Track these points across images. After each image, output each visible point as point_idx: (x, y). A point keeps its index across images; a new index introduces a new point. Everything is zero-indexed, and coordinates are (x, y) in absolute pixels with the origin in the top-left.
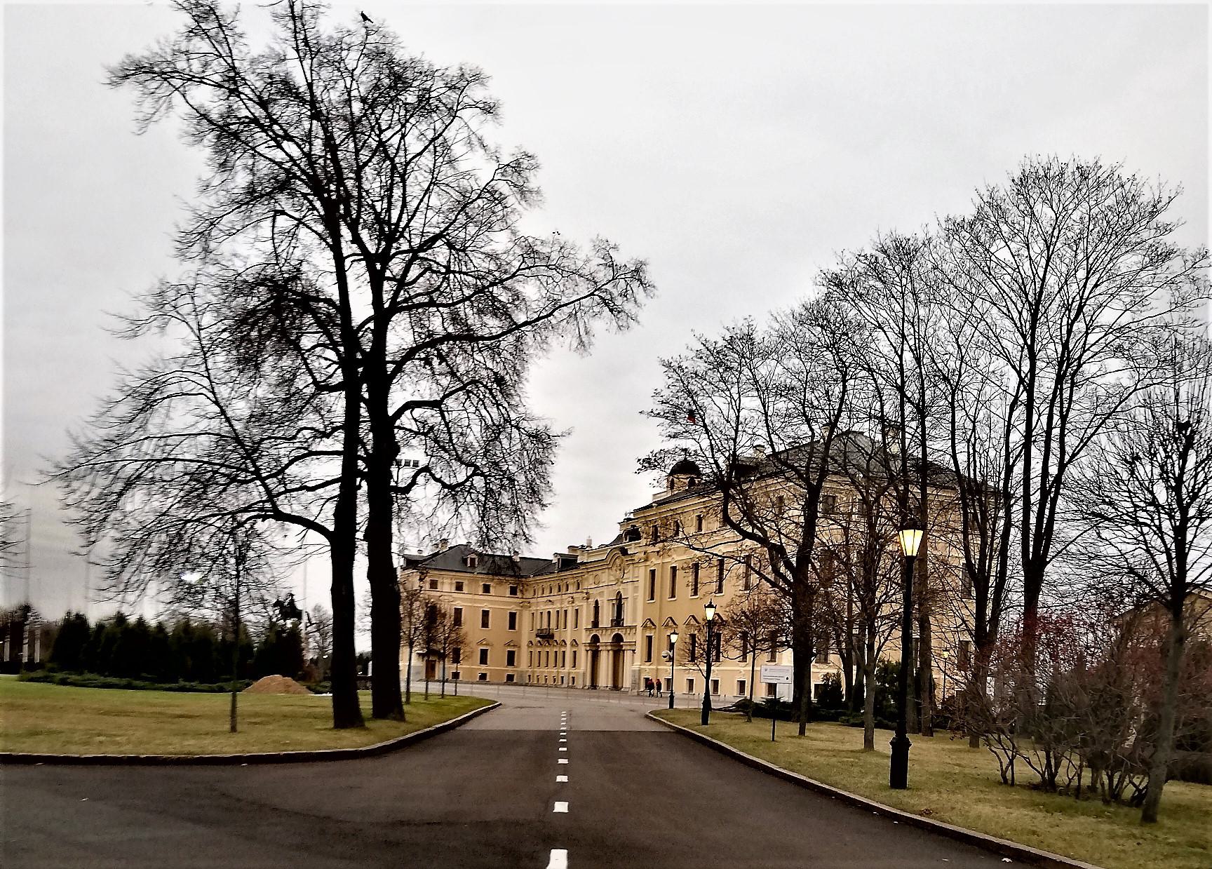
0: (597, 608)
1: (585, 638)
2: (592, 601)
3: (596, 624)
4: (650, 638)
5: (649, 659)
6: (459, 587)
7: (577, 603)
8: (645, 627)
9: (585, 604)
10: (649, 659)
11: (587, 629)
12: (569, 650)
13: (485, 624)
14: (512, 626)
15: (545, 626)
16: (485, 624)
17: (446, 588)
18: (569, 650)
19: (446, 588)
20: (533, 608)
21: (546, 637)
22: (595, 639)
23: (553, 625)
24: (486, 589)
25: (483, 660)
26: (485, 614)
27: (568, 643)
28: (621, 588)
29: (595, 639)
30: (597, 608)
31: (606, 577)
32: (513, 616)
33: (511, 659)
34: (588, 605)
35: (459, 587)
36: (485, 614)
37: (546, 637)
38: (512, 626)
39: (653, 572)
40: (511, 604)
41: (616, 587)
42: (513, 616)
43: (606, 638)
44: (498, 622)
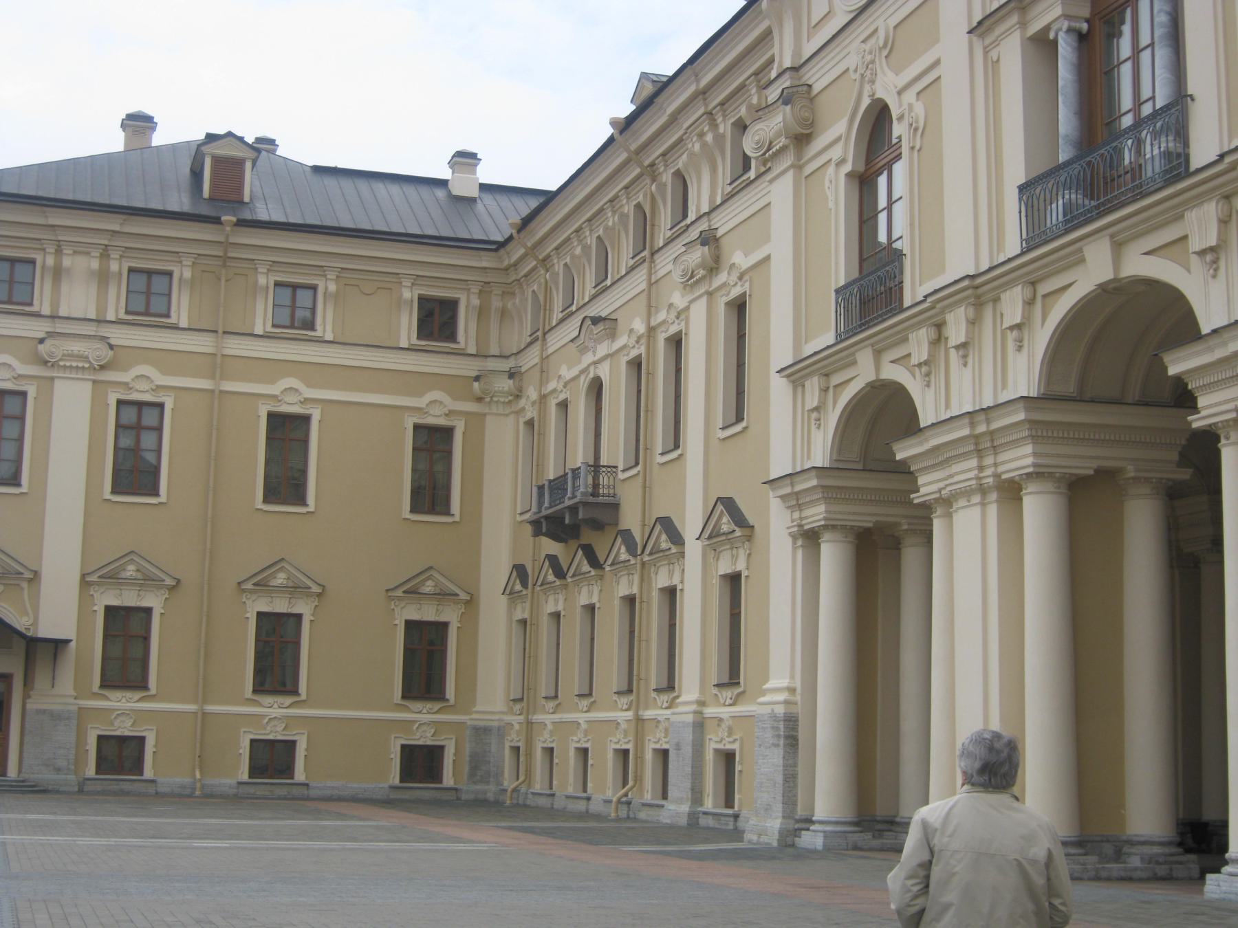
1: (794, 435)
12: (694, 576)
13: (286, 484)
14: (430, 495)
16: (286, 484)
17: (78, 298)
18: (694, 576)
19: (78, 298)
21: (576, 521)
22: (882, 419)
26: (287, 431)
27: (691, 525)
29: (882, 419)
32: (433, 442)
33: (425, 663)
34: (805, 182)
36: (287, 431)
37: (576, 521)
38: (430, 495)
40: (427, 387)
44: (359, 473)
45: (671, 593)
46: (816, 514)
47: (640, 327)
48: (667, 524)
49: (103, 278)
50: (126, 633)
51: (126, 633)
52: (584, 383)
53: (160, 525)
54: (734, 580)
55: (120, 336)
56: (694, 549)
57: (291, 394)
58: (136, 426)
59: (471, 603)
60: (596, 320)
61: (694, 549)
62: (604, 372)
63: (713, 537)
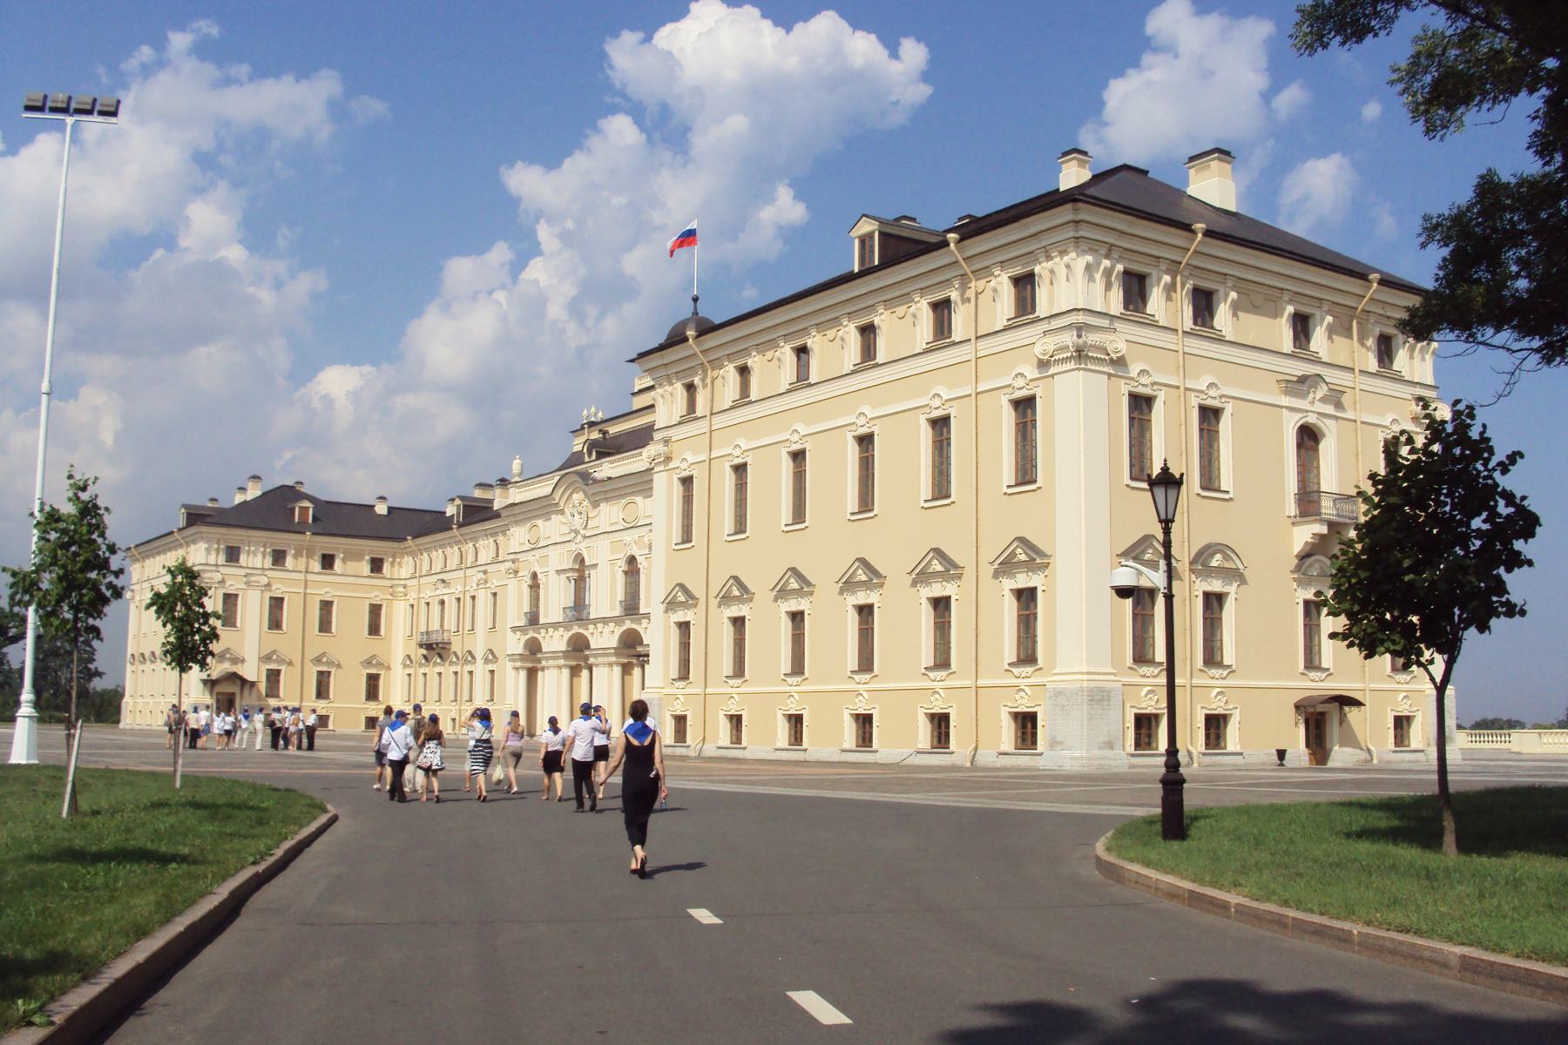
0: (535, 586)
1: (516, 644)
2: (525, 574)
3: (533, 619)
4: (684, 627)
5: (684, 675)
6: (279, 557)
7: (494, 582)
8: (671, 605)
9: (512, 583)
10: (684, 675)
11: (514, 629)
12: (481, 670)
13: (325, 626)
14: (374, 629)
15: (435, 626)
16: (325, 626)
20: (412, 595)
23: (450, 624)
24: (328, 561)
25: (322, 692)
26: (326, 606)
27: (479, 654)
28: (582, 547)
30: (535, 586)
31: (552, 528)
32: (375, 610)
35: (279, 557)
36: (326, 606)
38: (374, 629)
39: (687, 482)
41: (573, 546)
42: (375, 610)
43: (555, 642)
45: (471, 673)
46: (519, 664)
47: (460, 588)
48: (470, 652)
49: (264, 554)
50: (273, 676)
51: (273, 676)
52: (437, 599)
53: (286, 642)
54: (492, 672)
55: (270, 574)
56: (480, 661)
57: (327, 593)
58: (277, 603)
59: (389, 668)
60: (443, 581)
61: (480, 661)
62: (446, 598)
63: (487, 661)
